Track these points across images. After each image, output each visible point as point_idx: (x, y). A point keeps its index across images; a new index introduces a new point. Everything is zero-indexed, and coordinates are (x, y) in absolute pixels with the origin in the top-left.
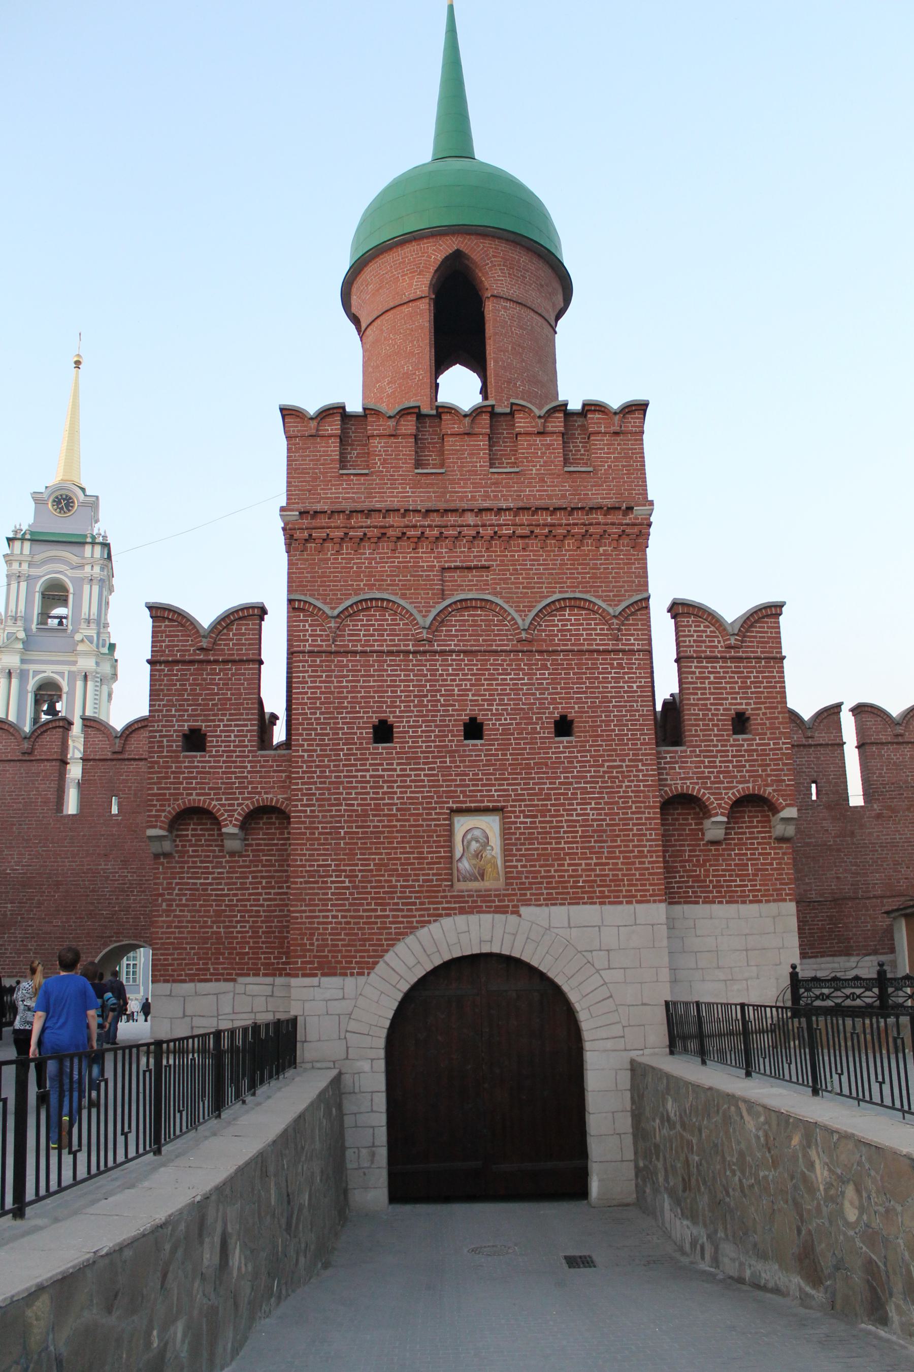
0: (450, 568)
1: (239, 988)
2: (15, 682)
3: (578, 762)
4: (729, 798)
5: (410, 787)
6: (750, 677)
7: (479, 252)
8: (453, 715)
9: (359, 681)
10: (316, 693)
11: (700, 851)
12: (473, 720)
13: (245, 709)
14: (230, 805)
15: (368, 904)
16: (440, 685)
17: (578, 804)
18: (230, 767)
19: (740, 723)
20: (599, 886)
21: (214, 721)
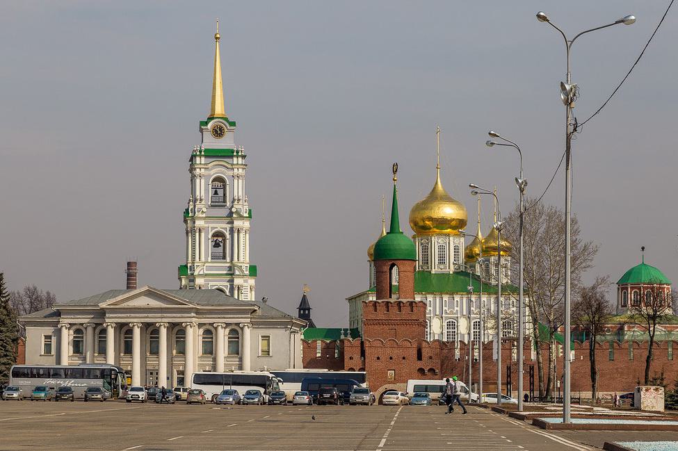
19: (431, 358)
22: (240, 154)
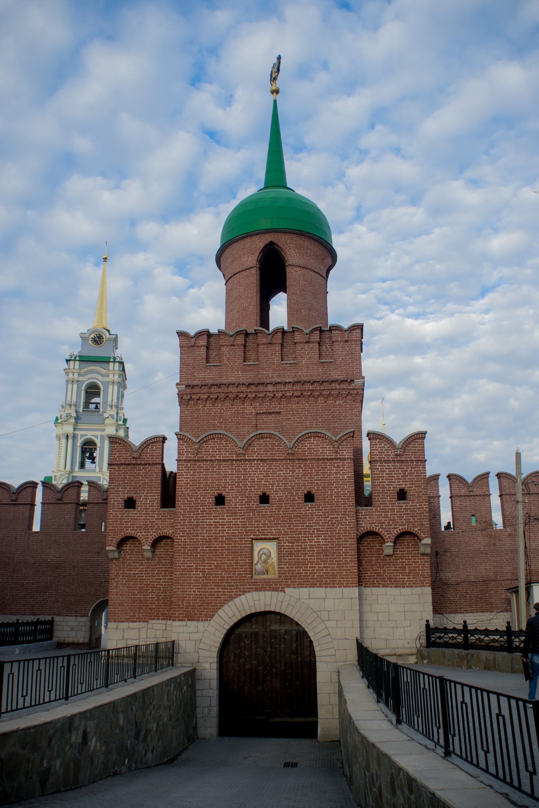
0: (260, 413)
1: (150, 626)
2: (70, 441)
3: (316, 515)
4: (395, 533)
5: (232, 527)
6: (407, 471)
8: (254, 492)
9: (209, 475)
10: (188, 480)
11: (381, 560)
12: (264, 494)
13: (154, 488)
14: (146, 535)
15: (211, 586)
16: (248, 477)
17: (315, 537)
18: (147, 517)
19: (402, 495)
20: (324, 578)
21: (139, 493)
22: (116, 360)
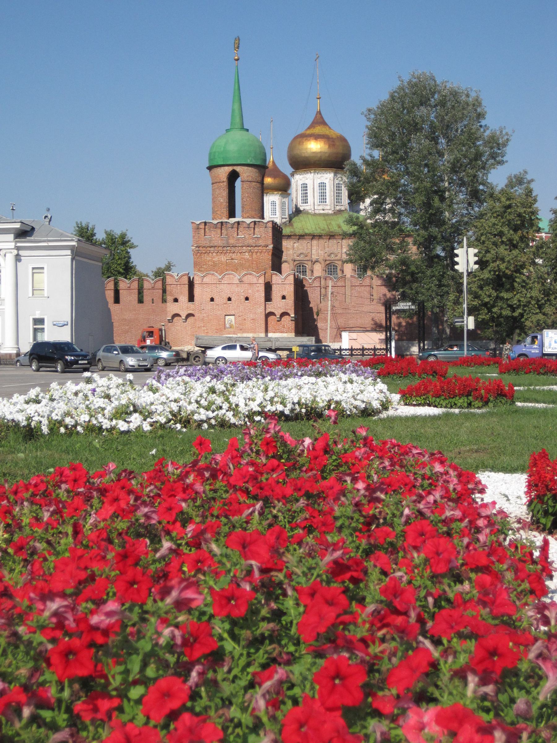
7: (238, 169)
